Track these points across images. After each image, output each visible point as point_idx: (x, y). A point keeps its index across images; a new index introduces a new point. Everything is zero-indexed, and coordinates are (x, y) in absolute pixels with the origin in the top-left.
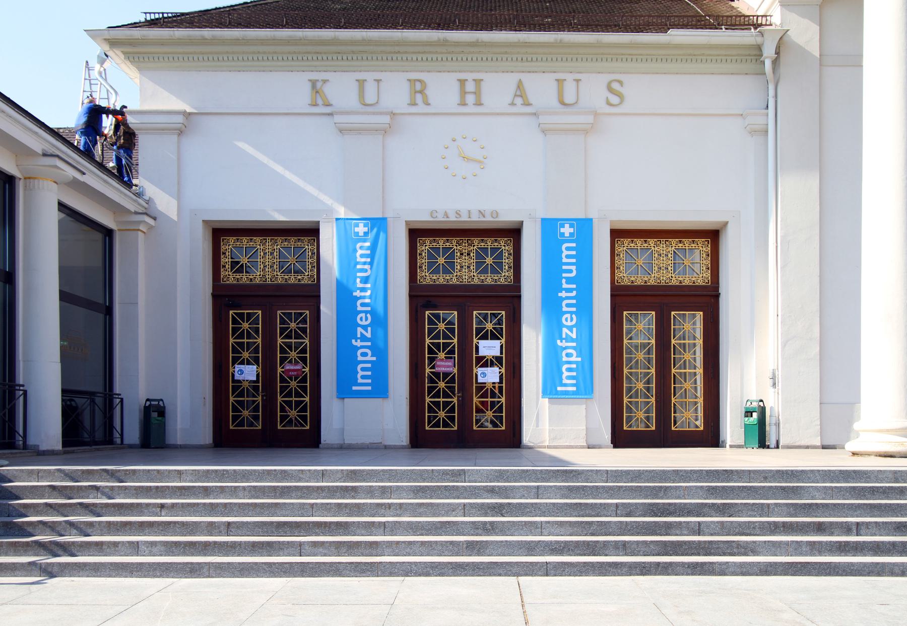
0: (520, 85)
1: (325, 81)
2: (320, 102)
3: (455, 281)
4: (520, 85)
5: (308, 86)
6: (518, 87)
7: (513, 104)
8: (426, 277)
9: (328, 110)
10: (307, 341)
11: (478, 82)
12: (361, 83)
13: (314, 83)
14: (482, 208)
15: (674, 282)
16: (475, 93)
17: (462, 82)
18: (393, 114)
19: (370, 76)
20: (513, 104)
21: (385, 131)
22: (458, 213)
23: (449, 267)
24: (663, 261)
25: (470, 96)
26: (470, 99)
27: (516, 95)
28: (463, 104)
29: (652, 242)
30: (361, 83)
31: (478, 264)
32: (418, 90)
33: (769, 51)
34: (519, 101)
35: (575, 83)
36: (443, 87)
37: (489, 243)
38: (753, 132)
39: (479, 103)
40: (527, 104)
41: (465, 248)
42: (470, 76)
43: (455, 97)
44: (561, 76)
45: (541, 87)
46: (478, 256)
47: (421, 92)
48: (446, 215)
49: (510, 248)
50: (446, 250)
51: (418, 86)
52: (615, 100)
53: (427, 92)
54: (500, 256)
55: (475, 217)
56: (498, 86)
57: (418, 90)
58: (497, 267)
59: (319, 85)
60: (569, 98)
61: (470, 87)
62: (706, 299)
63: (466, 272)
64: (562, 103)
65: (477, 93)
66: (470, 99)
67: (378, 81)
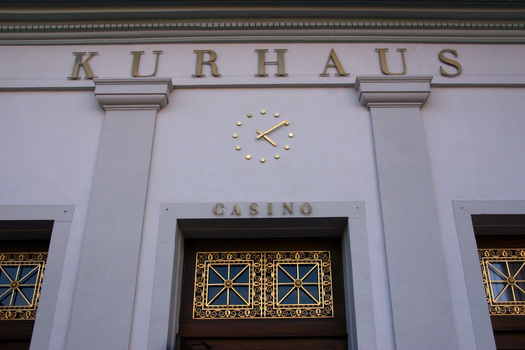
1: (93, 55)
5: (74, 58)
6: (331, 57)
7: (324, 75)
8: (205, 307)
9: (91, 84)
11: (281, 53)
12: (137, 56)
13: (79, 56)
14: (287, 200)
16: (277, 64)
17: (261, 53)
18: (173, 88)
20: (324, 75)
21: (161, 104)
26: (271, 70)
27: (328, 66)
30: (137, 56)
32: (207, 62)
34: (332, 71)
35: (399, 54)
41: (263, 266)
42: (272, 47)
46: (283, 276)
47: (208, 63)
50: (235, 268)
51: (207, 58)
54: (314, 276)
56: (305, 59)
57: (207, 62)
65: (280, 63)
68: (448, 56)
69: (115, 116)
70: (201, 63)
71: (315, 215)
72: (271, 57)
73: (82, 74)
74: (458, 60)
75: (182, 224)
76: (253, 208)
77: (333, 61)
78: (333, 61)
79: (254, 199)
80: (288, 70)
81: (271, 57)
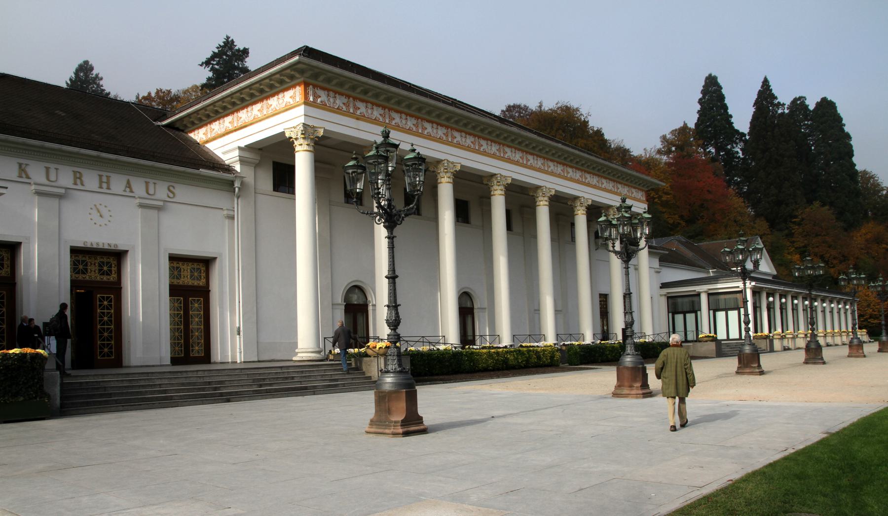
1: (27, 165)
3: (87, 278)
7: (125, 191)
11: (108, 177)
13: (20, 165)
15: (190, 284)
17: (101, 176)
18: (67, 188)
19: (52, 166)
20: (125, 191)
22: (97, 244)
23: (85, 271)
24: (185, 273)
25: (105, 185)
26: (105, 185)
28: (101, 187)
29: (181, 263)
31: (100, 270)
33: (237, 184)
34: (128, 190)
36: (91, 179)
37: (105, 260)
39: (108, 188)
40: (132, 191)
42: (104, 174)
43: (97, 185)
44: (148, 180)
45: (139, 186)
46: (100, 266)
47: (80, 178)
49: (115, 262)
50: (83, 261)
51: (78, 175)
52: (171, 195)
53: (83, 179)
54: (111, 266)
55: (106, 247)
56: (118, 182)
57: (78, 178)
58: (109, 273)
59: (23, 166)
61: (104, 179)
62: (204, 293)
64: (148, 193)
65: (108, 183)
66: (105, 185)
68: (171, 188)
70: (75, 178)
72: (104, 179)
73: (24, 176)
76: (97, 244)
77: (129, 185)
78: (129, 185)
80: (111, 187)
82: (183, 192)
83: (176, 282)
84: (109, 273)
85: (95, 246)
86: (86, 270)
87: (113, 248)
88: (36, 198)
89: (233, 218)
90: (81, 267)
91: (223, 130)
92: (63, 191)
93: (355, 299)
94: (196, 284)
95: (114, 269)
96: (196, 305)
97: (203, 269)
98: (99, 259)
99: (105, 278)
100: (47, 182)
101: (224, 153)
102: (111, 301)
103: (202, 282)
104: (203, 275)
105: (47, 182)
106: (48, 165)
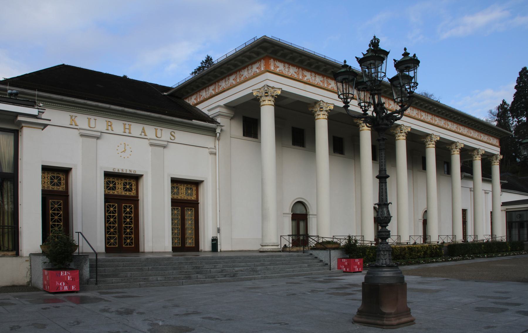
0: (143, 129)
2: (73, 124)
3: (116, 193)
4: (143, 129)
7: (141, 135)
10: (62, 212)
11: (130, 125)
13: (71, 117)
15: (185, 198)
20: (141, 135)
23: (114, 188)
33: (218, 130)
34: (143, 134)
36: (118, 125)
37: (128, 181)
38: (211, 153)
41: (120, 182)
42: (127, 123)
45: (151, 131)
46: (124, 185)
48: (122, 170)
50: (113, 182)
51: (109, 124)
52: (173, 138)
54: (131, 185)
56: (136, 128)
58: (130, 190)
60: (159, 135)
62: (194, 205)
63: (120, 190)
67: (95, 120)
68: (173, 133)
69: (85, 139)
71: (137, 173)
73: (73, 124)
74: (174, 135)
75: (105, 172)
77: (143, 131)
78: (143, 131)
79: (122, 168)
81: (127, 127)
82: (182, 136)
83: (175, 197)
84: (130, 190)
85: (120, 171)
86: (115, 187)
87: (132, 173)
88: (81, 139)
89: (215, 154)
90: (111, 185)
91: (208, 95)
92: (99, 134)
93: (300, 210)
94: (189, 198)
95: (134, 187)
96: (189, 214)
97: (194, 188)
98: (124, 181)
99: (128, 193)
100: (89, 128)
101: (209, 110)
102: (131, 209)
103: (193, 198)
104: (194, 192)
105: (89, 128)
106: (89, 117)
